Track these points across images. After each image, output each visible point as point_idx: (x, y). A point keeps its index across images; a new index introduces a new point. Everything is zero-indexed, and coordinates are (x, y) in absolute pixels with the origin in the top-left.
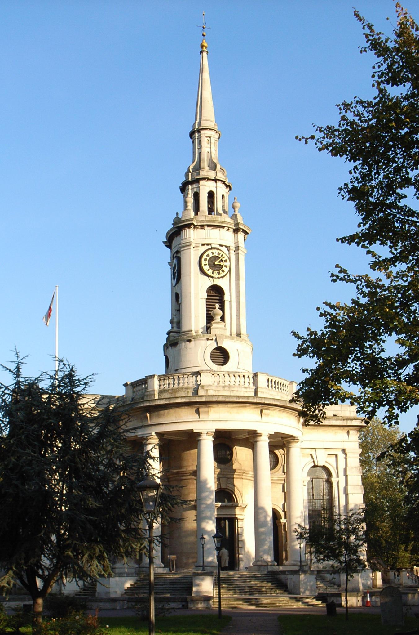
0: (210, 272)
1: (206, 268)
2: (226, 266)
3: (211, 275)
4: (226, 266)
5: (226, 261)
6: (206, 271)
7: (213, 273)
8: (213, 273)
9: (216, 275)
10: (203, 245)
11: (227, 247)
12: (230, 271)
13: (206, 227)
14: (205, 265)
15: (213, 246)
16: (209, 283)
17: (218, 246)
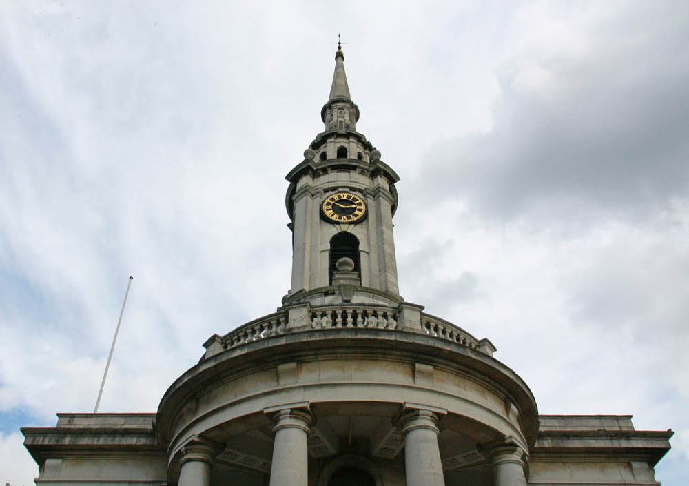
0: (335, 218)
1: (328, 213)
2: (361, 210)
3: (337, 220)
4: (361, 210)
5: (360, 204)
6: (330, 216)
7: (340, 218)
8: (340, 218)
9: (344, 219)
10: (326, 191)
11: (361, 191)
12: (365, 217)
13: (329, 171)
14: (327, 210)
15: (340, 190)
16: (333, 231)
17: (348, 190)
